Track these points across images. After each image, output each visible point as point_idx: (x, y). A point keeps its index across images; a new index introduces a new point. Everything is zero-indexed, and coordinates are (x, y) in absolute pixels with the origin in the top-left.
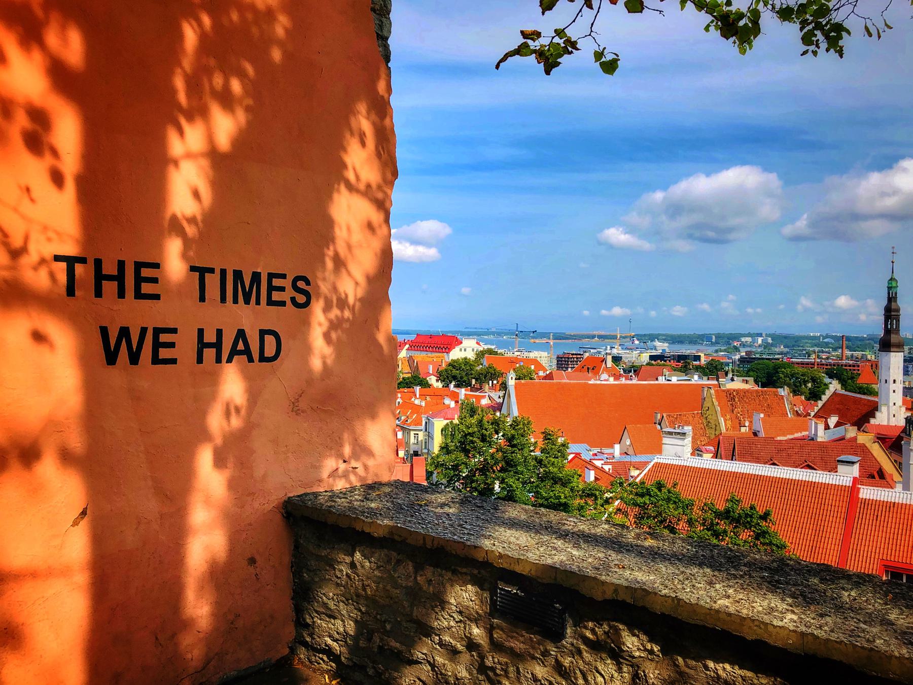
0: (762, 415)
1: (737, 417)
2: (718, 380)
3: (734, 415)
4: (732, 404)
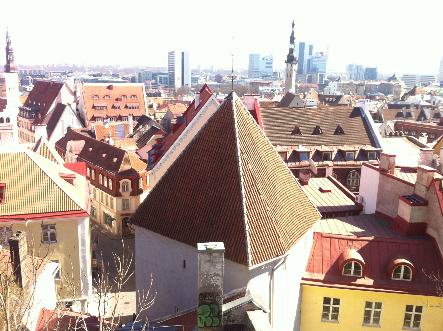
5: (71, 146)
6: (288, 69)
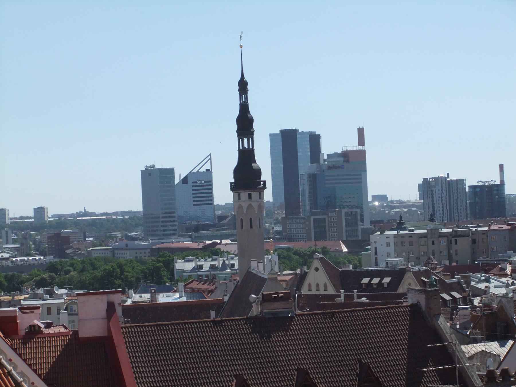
6: (240, 207)
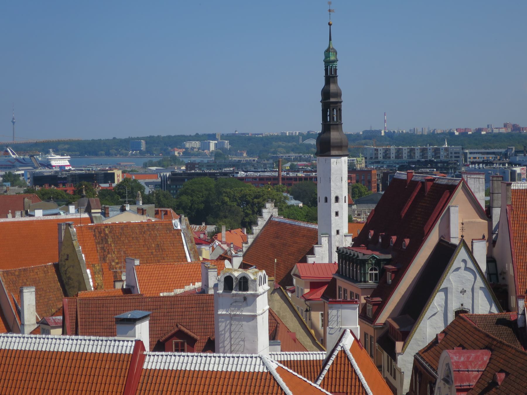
0: (137, 262)
1: (111, 267)
2: (90, 213)
3: (106, 264)
4: (102, 248)
5: (448, 365)
